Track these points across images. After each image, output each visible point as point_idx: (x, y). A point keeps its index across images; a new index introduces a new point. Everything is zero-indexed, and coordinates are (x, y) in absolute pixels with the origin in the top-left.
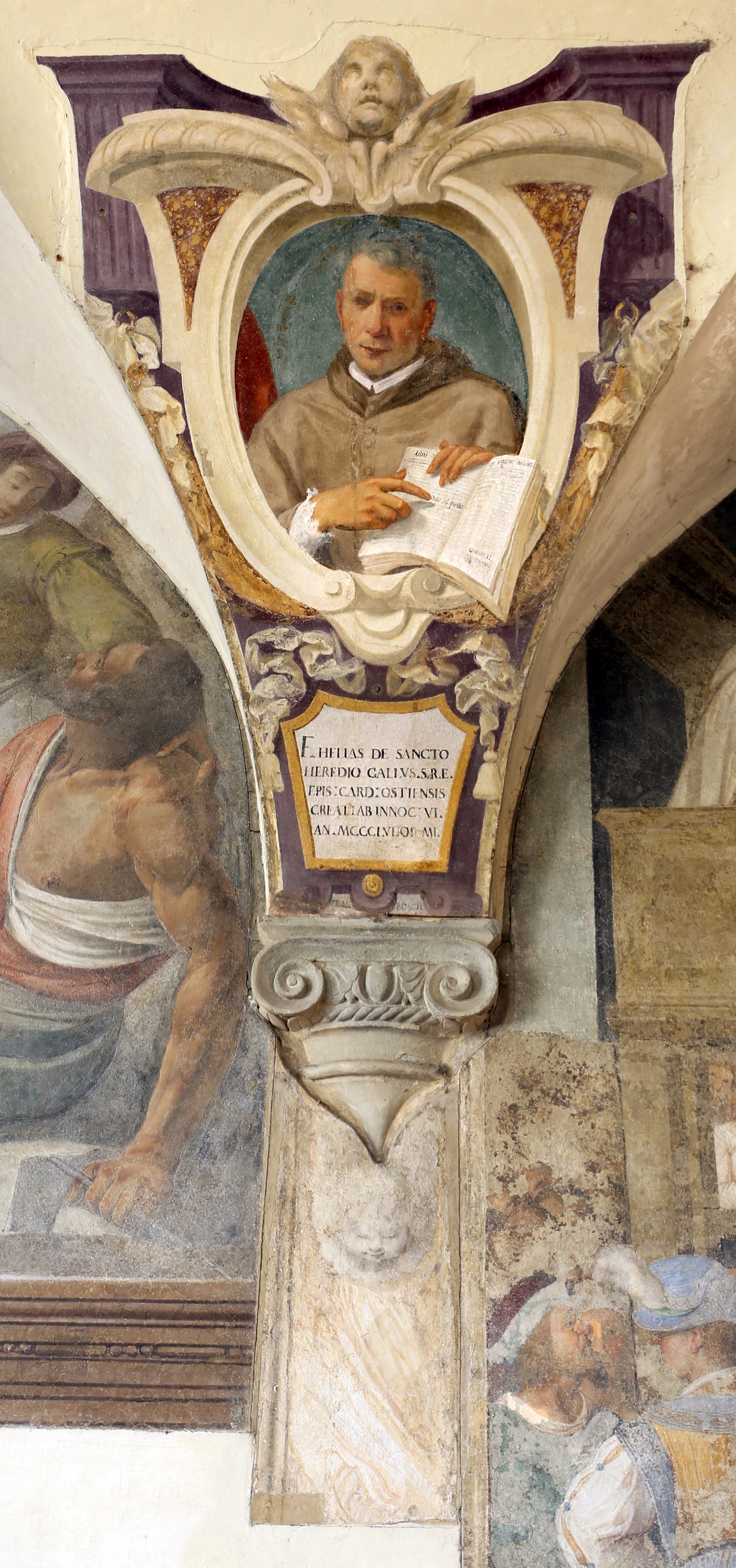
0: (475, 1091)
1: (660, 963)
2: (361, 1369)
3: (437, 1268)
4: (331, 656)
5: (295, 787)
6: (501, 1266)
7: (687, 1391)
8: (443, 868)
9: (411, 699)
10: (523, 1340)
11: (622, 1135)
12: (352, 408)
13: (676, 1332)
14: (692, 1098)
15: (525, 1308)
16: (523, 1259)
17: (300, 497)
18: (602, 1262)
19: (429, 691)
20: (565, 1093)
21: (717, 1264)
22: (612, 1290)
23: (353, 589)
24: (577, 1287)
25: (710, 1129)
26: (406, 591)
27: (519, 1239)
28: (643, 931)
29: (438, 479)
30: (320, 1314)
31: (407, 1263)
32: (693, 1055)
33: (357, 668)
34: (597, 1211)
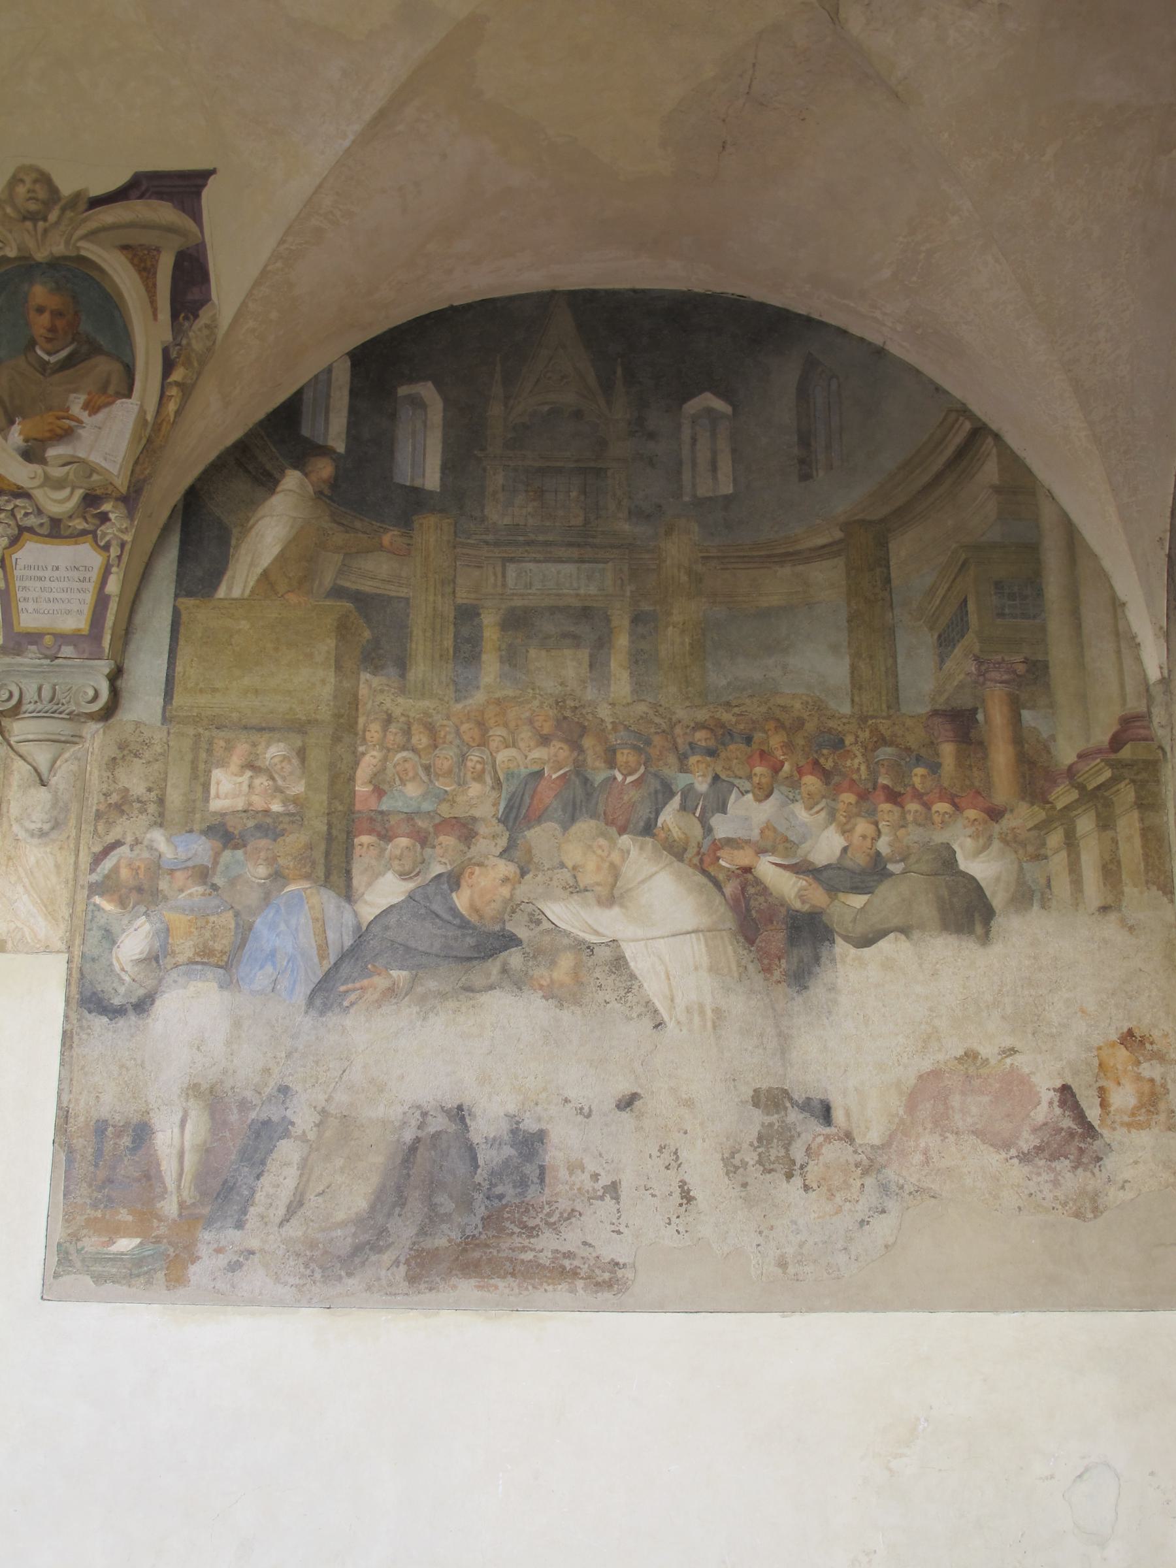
0: (96, 750)
1: (197, 684)
2: (28, 884)
3: (68, 837)
4: (31, 513)
5: (11, 586)
6: (100, 837)
7: (180, 897)
8: (86, 632)
9: (74, 537)
10: (106, 872)
11: (166, 773)
12: (38, 371)
13: (179, 869)
14: (203, 755)
15: (108, 857)
16: (111, 834)
17: (12, 422)
18: (148, 836)
19: (84, 533)
20: (141, 752)
21: (204, 838)
22: (152, 849)
23: (43, 475)
24: (135, 848)
25: (210, 771)
26: (71, 476)
27: (110, 824)
28: (192, 667)
29: (86, 413)
30: (10, 858)
31: (54, 835)
32: (207, 733)
33: (45, 520)
34: (149, 811)
